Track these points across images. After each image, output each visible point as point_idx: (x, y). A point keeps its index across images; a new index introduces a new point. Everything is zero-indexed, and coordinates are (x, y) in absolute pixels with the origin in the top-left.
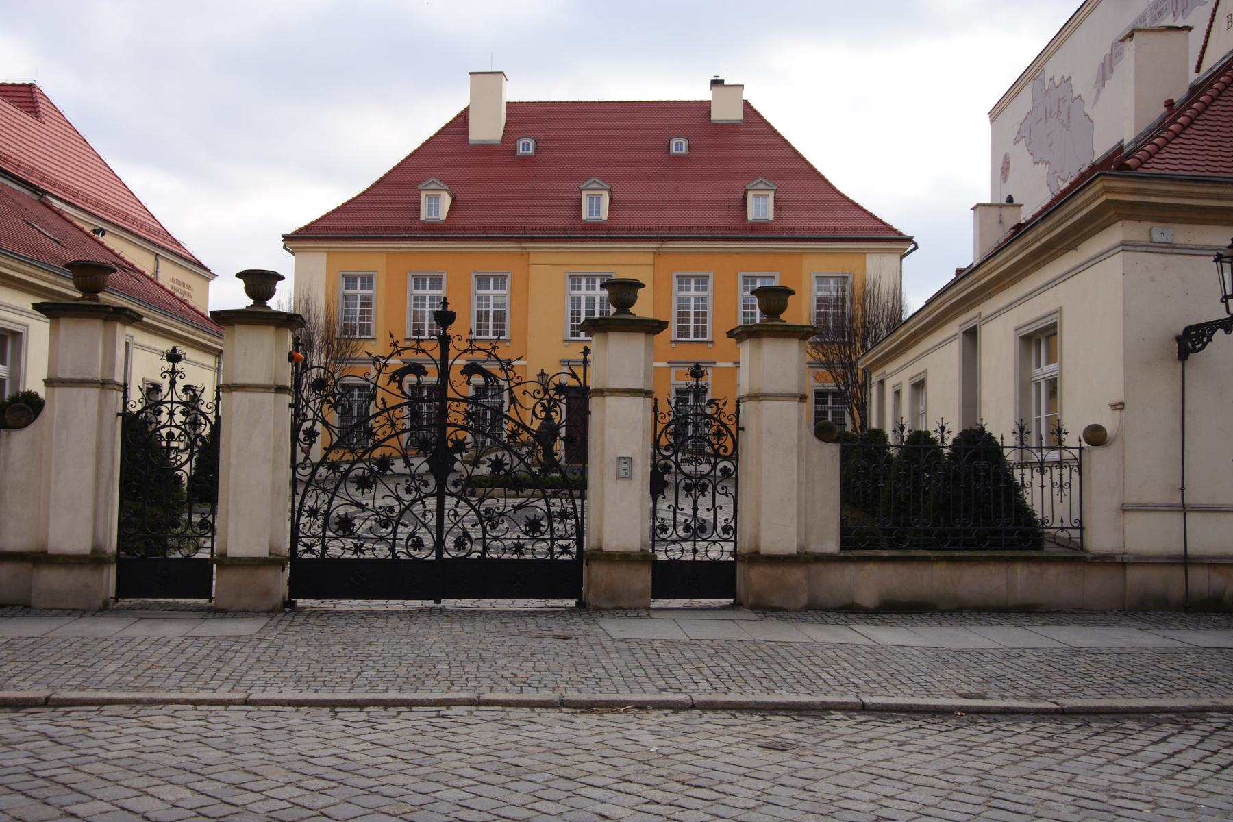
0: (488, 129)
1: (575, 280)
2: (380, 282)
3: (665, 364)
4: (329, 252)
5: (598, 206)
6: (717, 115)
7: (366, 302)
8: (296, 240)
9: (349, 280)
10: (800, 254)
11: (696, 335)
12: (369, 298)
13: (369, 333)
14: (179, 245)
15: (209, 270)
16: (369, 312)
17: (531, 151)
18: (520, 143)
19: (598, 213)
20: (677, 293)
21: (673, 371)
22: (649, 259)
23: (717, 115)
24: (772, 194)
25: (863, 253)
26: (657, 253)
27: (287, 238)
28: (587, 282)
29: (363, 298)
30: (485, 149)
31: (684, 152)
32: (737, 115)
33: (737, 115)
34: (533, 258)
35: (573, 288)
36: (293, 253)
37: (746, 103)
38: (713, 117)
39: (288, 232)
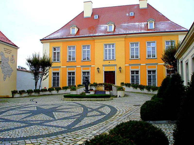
0: (88, 14)
1: (106, 45)
2: (61, 49)
3: (128, 65)
4: (50, 42)
5: (111, 28)
6: (141, 7)
7: (58, 53)
8: (43, 40)
9: (55, 49)
10: (162, 36)
11: (136, 57)
12: (59, 52)
13: (59, 61)
14: (10, 41)
15: (17, 47)
16: (59, 56)
17: (97, 18)
18: (95, 16)
19: (111, 30)
20: (131, 47)
21: (130, 66)
22: (124, 39)
23: (141, 7)
24: (154, 22)
25: (178, 35)
26: (125, 38)
27: (41, 40)
28: (109, 46)
29: (58, 53)
30: (87, 18)
31: (133, 15)
32: (146, 6)
33: (146, 6)
34: (95, 41)
35: (106, 48)
36: (43, 43)
37: (148, 4)
38: (140, 7)
39: (41, 38)
